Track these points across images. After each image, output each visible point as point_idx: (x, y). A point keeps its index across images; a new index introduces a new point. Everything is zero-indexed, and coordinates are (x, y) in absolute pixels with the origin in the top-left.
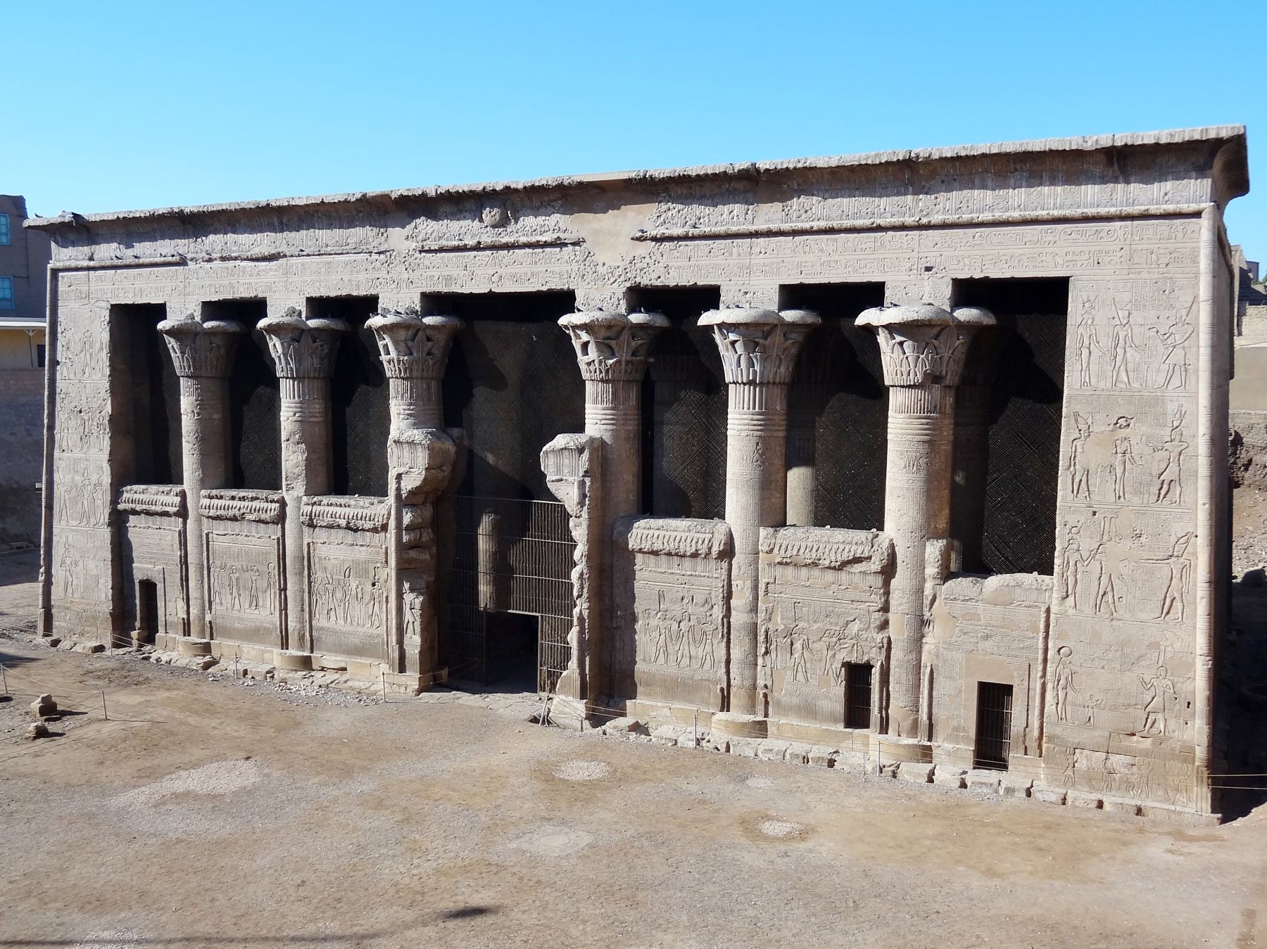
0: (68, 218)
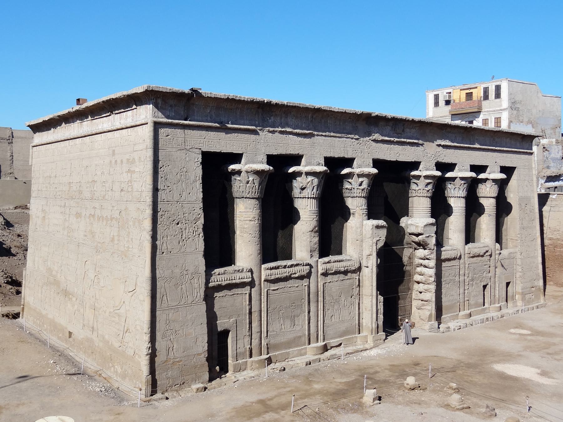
0: (187, 90)
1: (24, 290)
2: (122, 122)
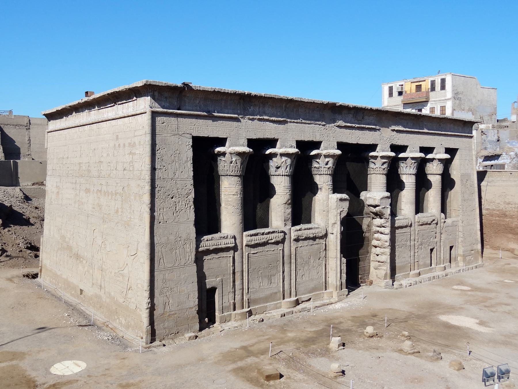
0: (179, 84)
1: (42, 254)
2: (124, 111)
